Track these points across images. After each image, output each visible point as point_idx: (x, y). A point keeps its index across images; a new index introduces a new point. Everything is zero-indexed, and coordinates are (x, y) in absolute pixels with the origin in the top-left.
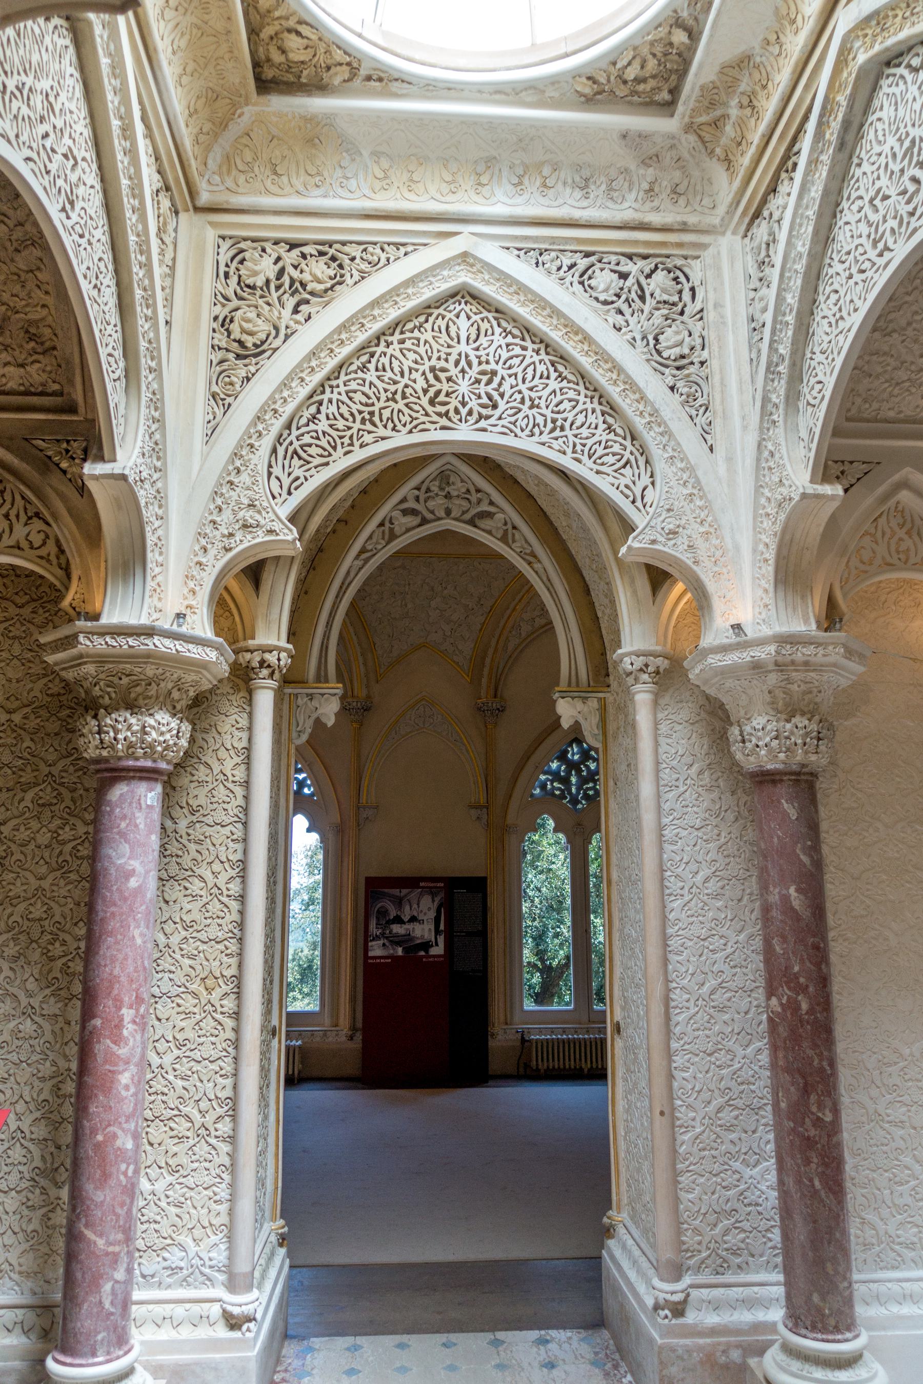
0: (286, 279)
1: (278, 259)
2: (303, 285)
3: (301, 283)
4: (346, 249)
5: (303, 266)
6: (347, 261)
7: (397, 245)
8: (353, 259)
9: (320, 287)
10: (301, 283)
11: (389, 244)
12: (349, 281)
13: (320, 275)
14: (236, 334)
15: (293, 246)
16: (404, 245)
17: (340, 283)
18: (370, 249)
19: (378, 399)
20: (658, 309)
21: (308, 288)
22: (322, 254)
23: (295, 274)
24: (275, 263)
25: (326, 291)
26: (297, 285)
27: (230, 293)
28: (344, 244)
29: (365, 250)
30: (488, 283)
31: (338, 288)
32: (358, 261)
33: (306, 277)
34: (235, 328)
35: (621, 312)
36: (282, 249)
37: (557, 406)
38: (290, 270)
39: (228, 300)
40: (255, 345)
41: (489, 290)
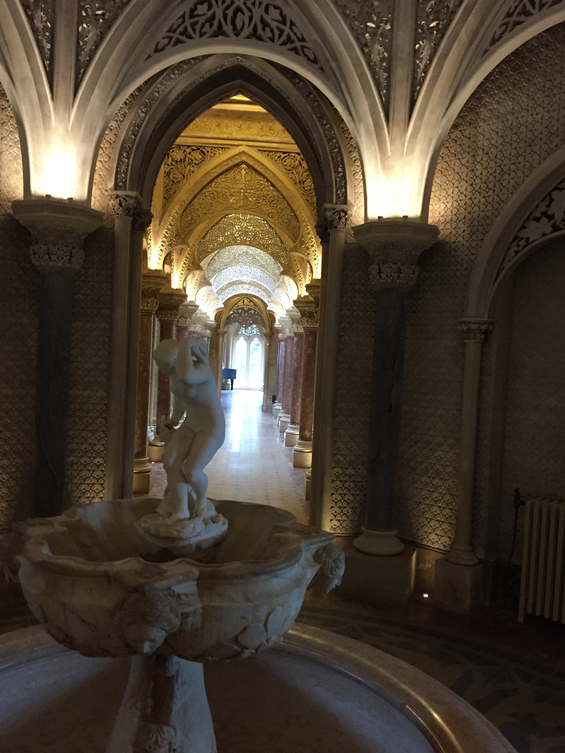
0: (187, 159)
1: (185, 151)
2: (192, 161)
3: (191, 159)
4: (206, 148)
5: (192, 153)
6: (206, 153)
7: (222, 148)
8: (208, 152)
9: (197, 162)
10: (191, 159)
11: (220, 148)
12: (206, 160)
13: (198, 158)
14: (172, 178)
15: (189, 146)
16: (225, 148)
17: (203, 161)
18: (214, 149)
19: (215, 198)
20: (305, 172)
21: (193, 162)
22: (198, 149)
23: (190, 156)
24: (184, 152)
25: (199, 163)
26: (190, 160)
27: (169, 163)
28: (205, 147)
29: (212, 149)
30: (251, 161)
31: (203, 162)
32: (209, 153)
33: (193, 159)
34: (171, 176)
35: (293, 173)
36: (185, 148)
37: (272, 202)
38: (188, 155)
39: (168, 165)
40: (177, 182)
41: (251, 163)
